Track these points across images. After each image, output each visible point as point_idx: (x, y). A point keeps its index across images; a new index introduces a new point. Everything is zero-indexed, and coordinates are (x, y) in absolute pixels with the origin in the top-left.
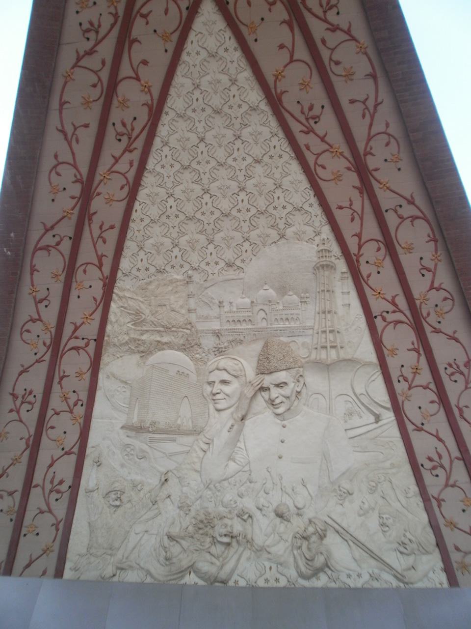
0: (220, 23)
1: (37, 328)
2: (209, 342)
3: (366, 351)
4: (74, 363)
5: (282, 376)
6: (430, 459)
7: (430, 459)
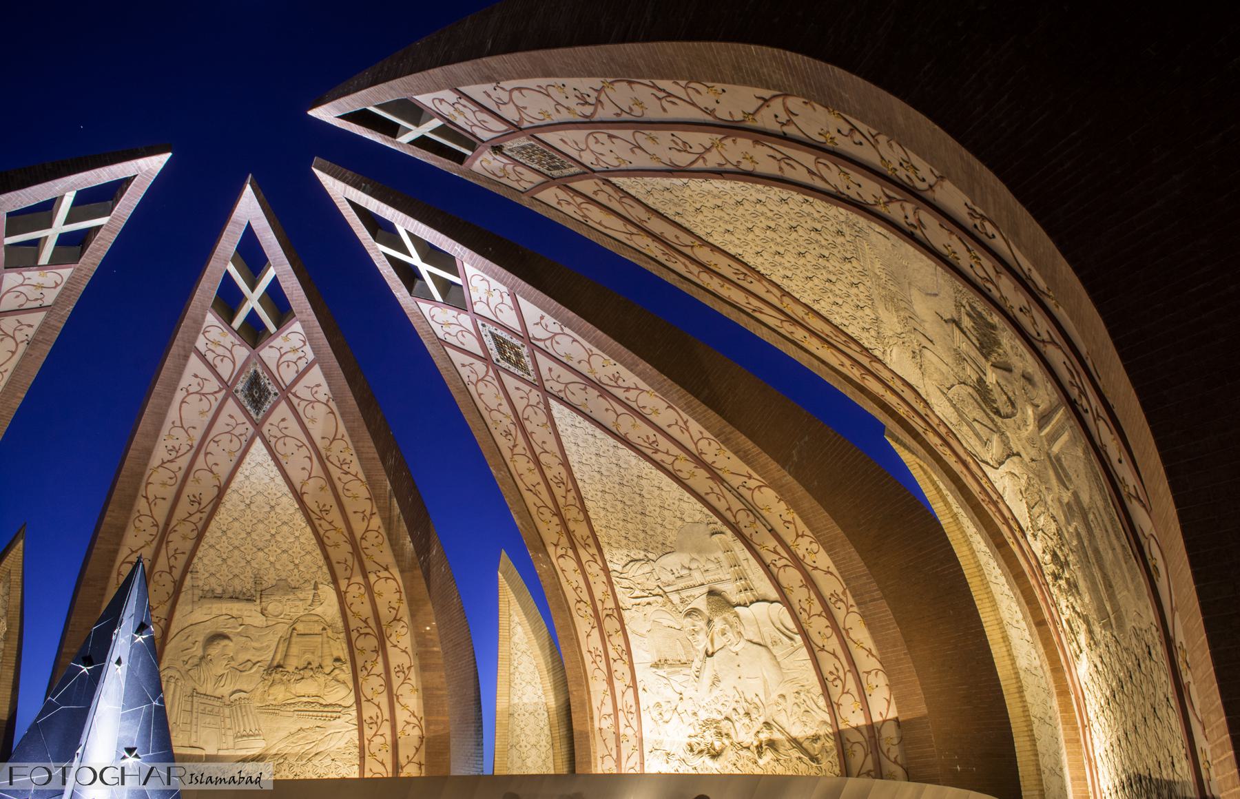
0: (567, 411)
1: (581, 605)
4: (611, 625)
6: (831, 673)
7: (831, 673)
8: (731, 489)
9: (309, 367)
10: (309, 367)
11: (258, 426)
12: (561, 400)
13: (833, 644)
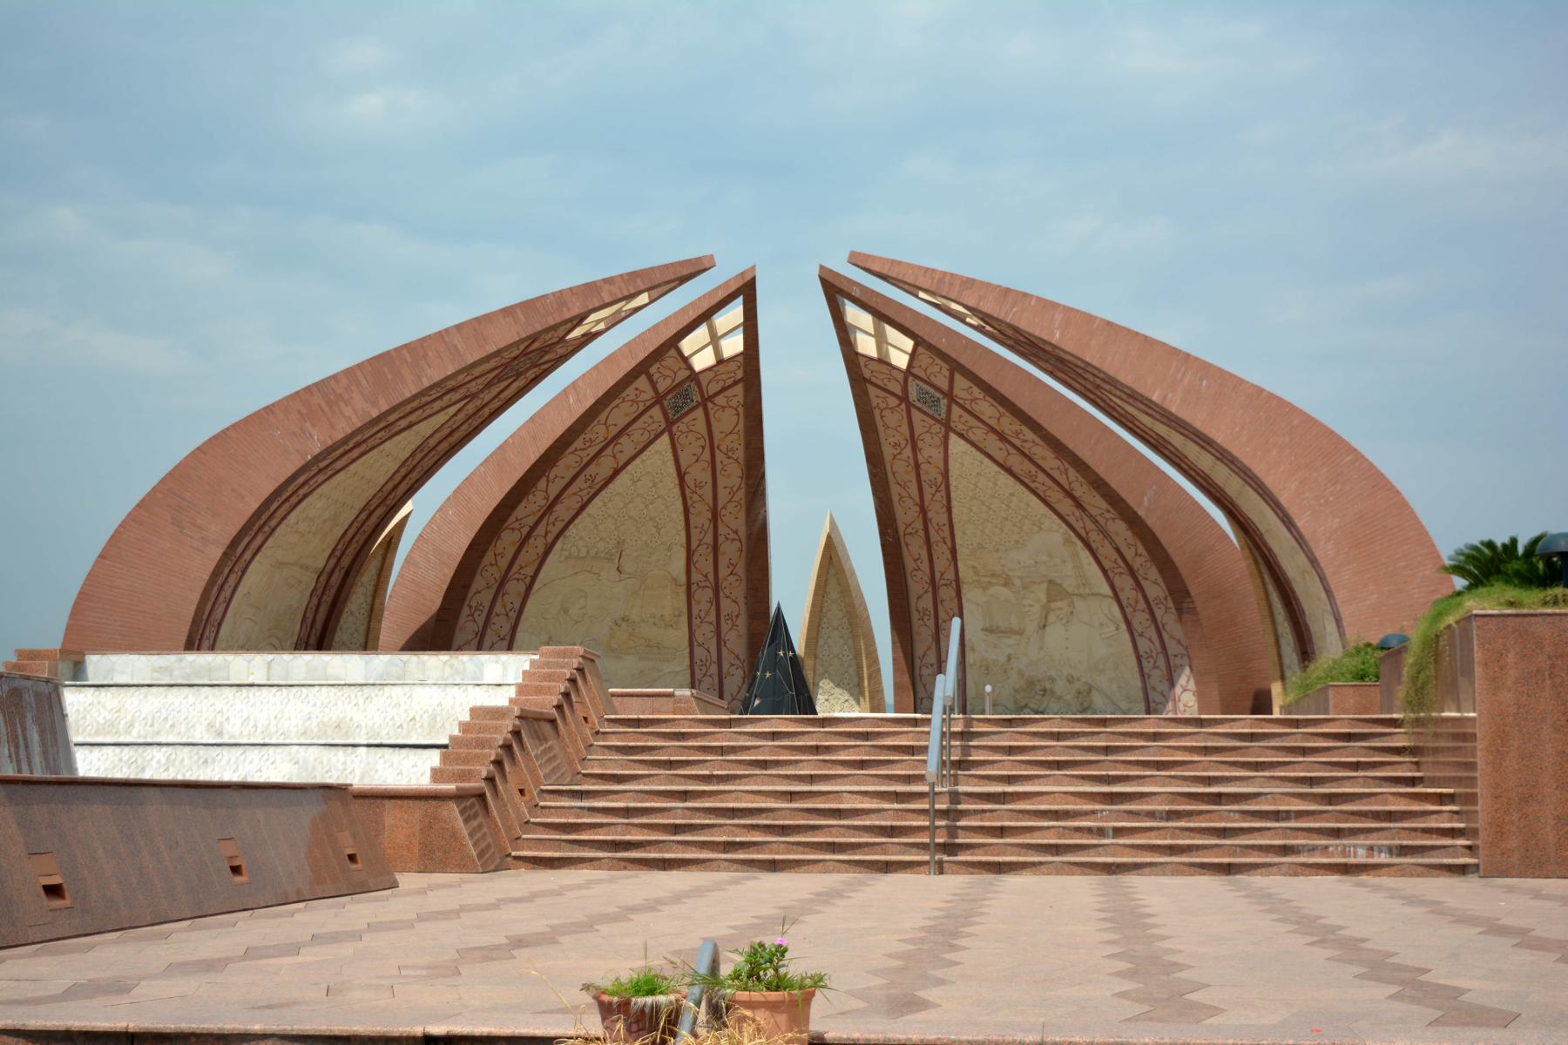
0: (963, 442)
1: (919, 574)
2: (1017, 582)
3: (1105, 589)
5: (1059, 604)
8: (1091, 517)
9: (735, 383)
10: (735, 383)
11: (670, 424)
12: (961, 436)
13: (1152, 632)
